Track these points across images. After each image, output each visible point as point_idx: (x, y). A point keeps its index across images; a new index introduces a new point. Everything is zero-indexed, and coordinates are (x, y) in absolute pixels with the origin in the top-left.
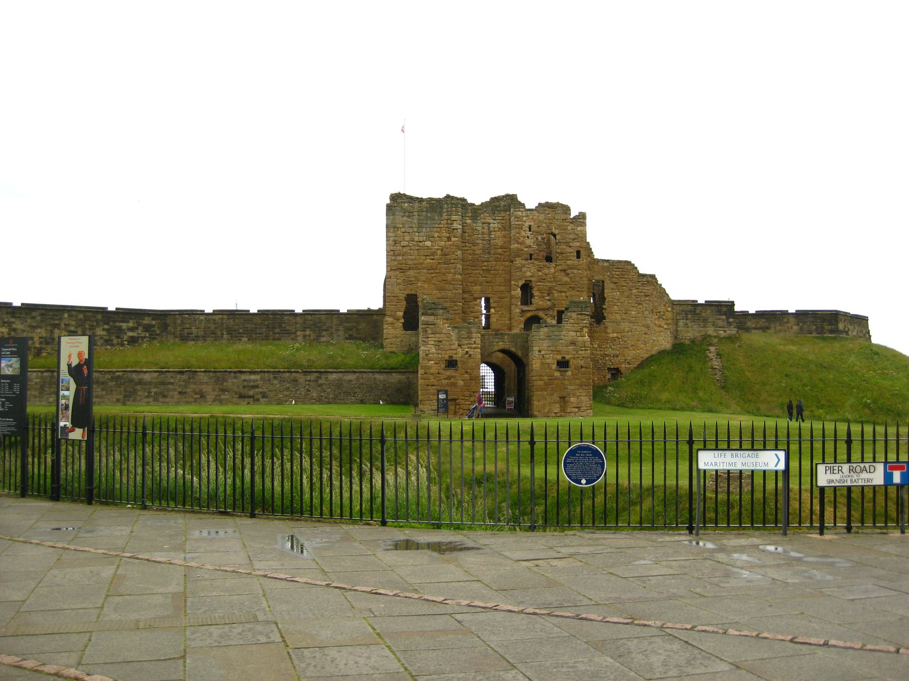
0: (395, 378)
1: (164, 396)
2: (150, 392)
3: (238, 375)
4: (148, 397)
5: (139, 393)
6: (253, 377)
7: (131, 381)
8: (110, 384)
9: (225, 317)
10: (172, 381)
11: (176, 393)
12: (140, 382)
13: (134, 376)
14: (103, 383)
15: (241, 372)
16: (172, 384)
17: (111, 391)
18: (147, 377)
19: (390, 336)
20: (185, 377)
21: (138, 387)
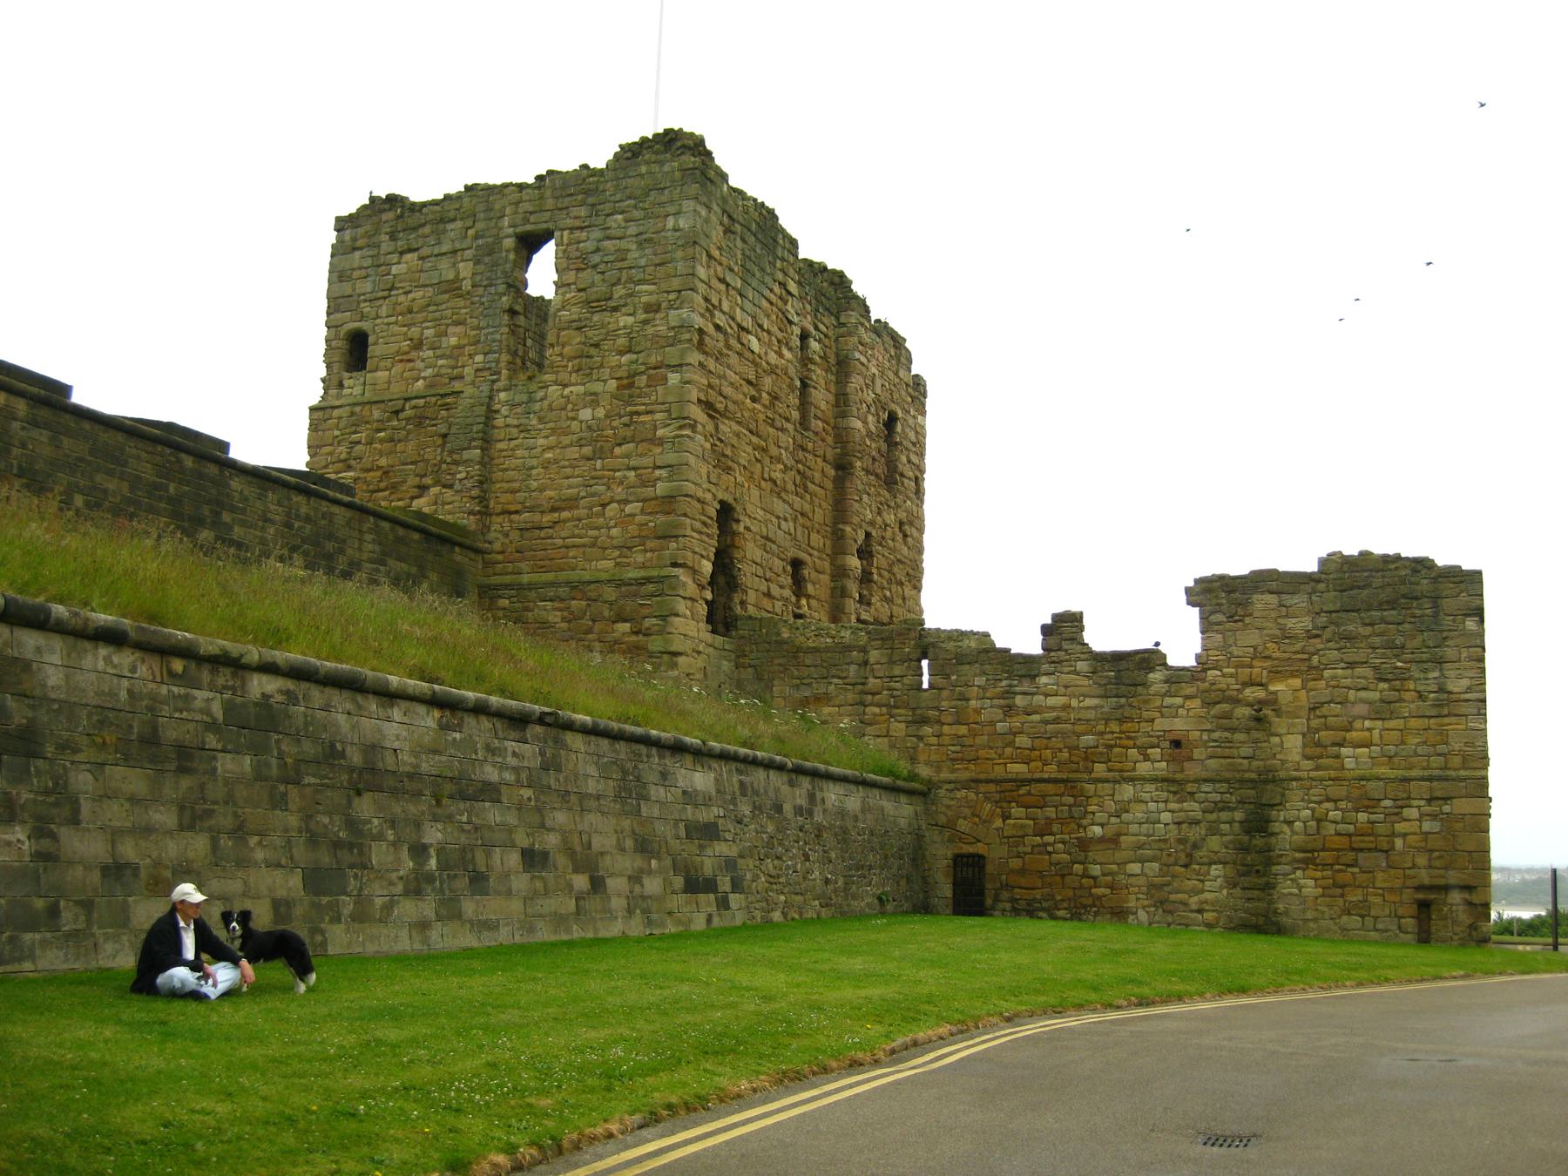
0: (902, 811)
1: (479, 882)
2: (419, 851)
3: (654, 762)
4: (415, 888)
5: (379, 854)
7: (332, 754)
8: (227, 764)
9: (21, 406)
10: (491, 774)
11: (514, 859)
12: (371, 775)
14: (186, 757)
15: (678, 748)
16: (490, 792)
17: (240, 832)
19: (686, 646)
21: (365, 807)
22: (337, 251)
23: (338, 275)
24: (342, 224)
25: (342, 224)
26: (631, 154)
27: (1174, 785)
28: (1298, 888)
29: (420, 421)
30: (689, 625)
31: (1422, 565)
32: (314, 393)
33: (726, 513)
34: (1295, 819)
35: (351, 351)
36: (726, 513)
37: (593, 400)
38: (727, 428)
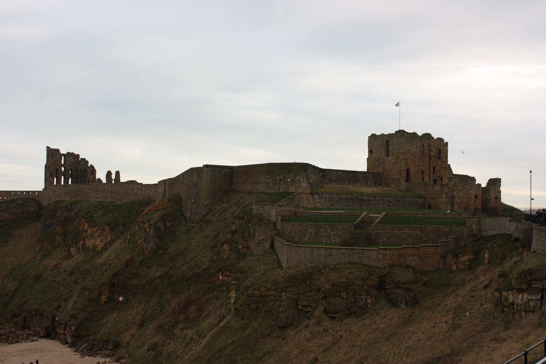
0: (421, 200)
6: (390, 199)
13: (361, 197)
18: (364, 197)
20: (374, 198)
22: (369, 140)
23: (369, 143)
24: (369, 137)
25: (369, 137)
26: (396, 132)
27: (446, 198)
28: (456, 207)
29: (378, 160)
30: (403, 182)
31: (467, 176)
32: (367, 157)
33: (408, 170)
34: (456, 200)
35: (370, 152)
36: (408, 170)
37: (393, 159)
38: (408, 161)
